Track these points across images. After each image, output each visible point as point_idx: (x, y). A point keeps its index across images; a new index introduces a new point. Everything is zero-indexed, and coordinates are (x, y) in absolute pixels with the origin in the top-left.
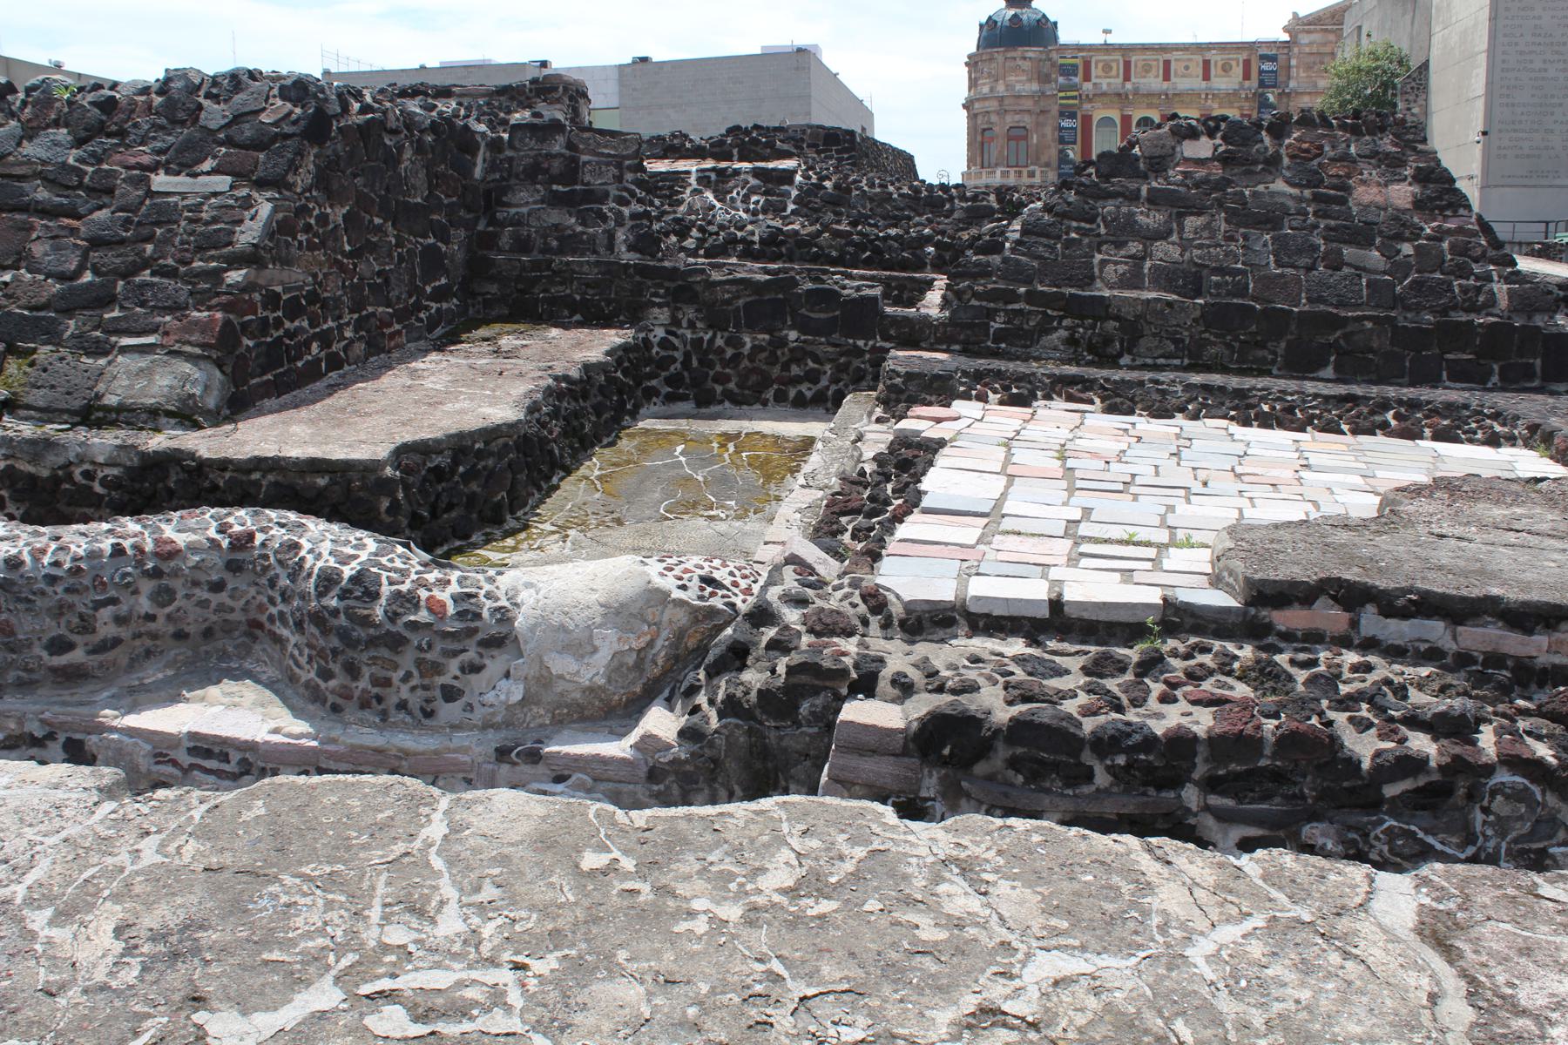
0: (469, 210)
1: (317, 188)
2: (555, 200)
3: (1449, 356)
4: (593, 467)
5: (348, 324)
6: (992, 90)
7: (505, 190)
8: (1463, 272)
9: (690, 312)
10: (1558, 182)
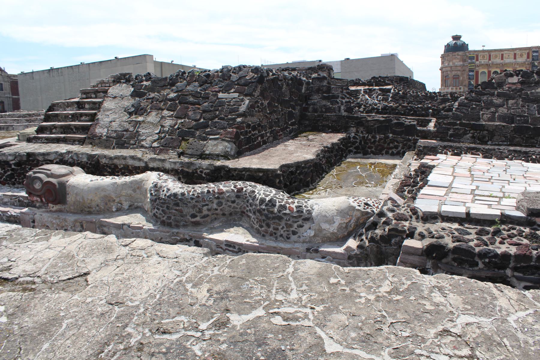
0: (301, 101)
1: (261, 96)
2: (324, 98)
4: (334, 172)
5: (268, 132)
6: (448, 64)
7: (311, 96)
9: (361, 129)
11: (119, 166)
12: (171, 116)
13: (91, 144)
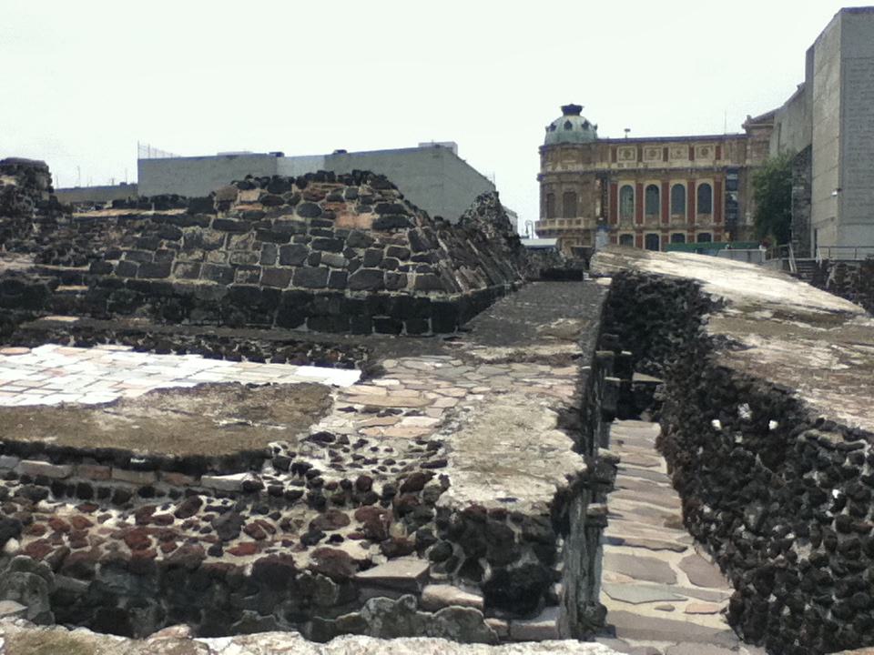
3: (374, 317)
6: (553, 169)
8: (393, 265)
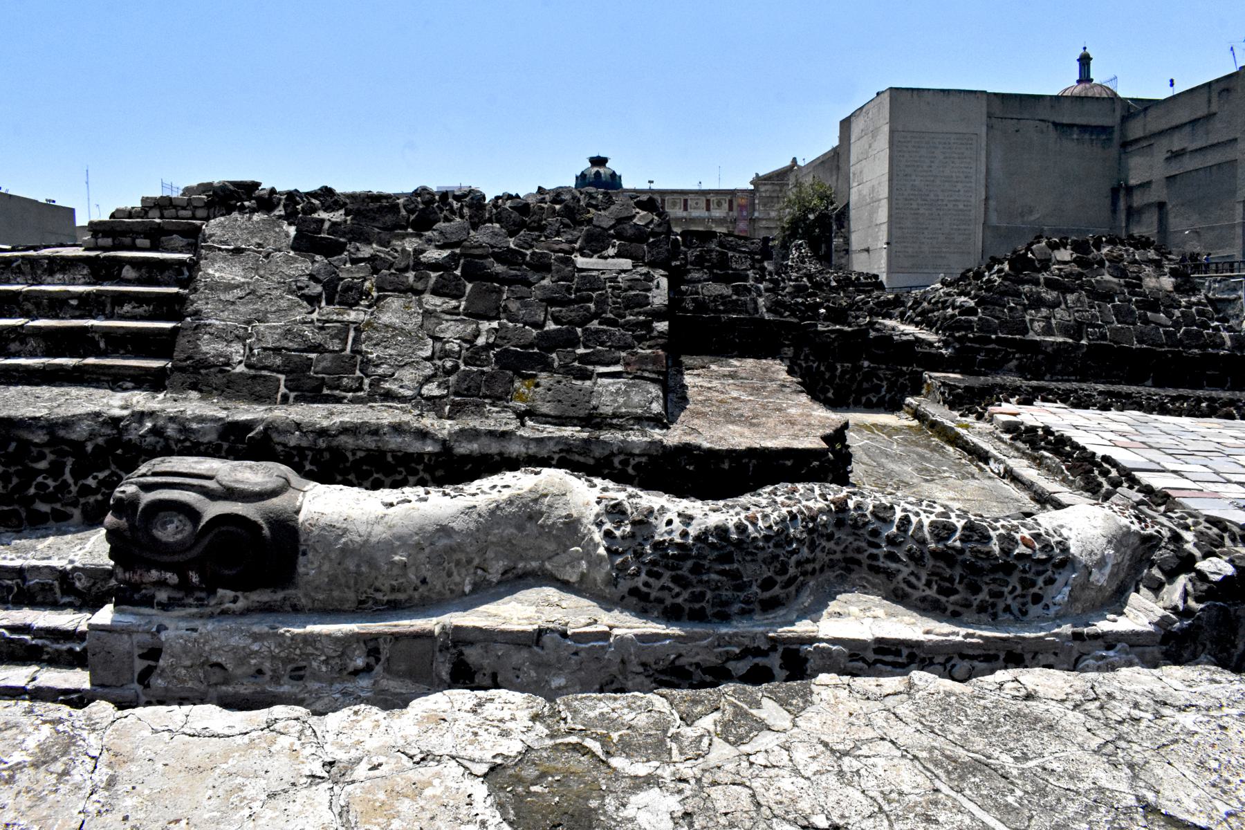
10: (926, 271)
11: (349, 454)
12: (454, 312)
13: (194, 387)
